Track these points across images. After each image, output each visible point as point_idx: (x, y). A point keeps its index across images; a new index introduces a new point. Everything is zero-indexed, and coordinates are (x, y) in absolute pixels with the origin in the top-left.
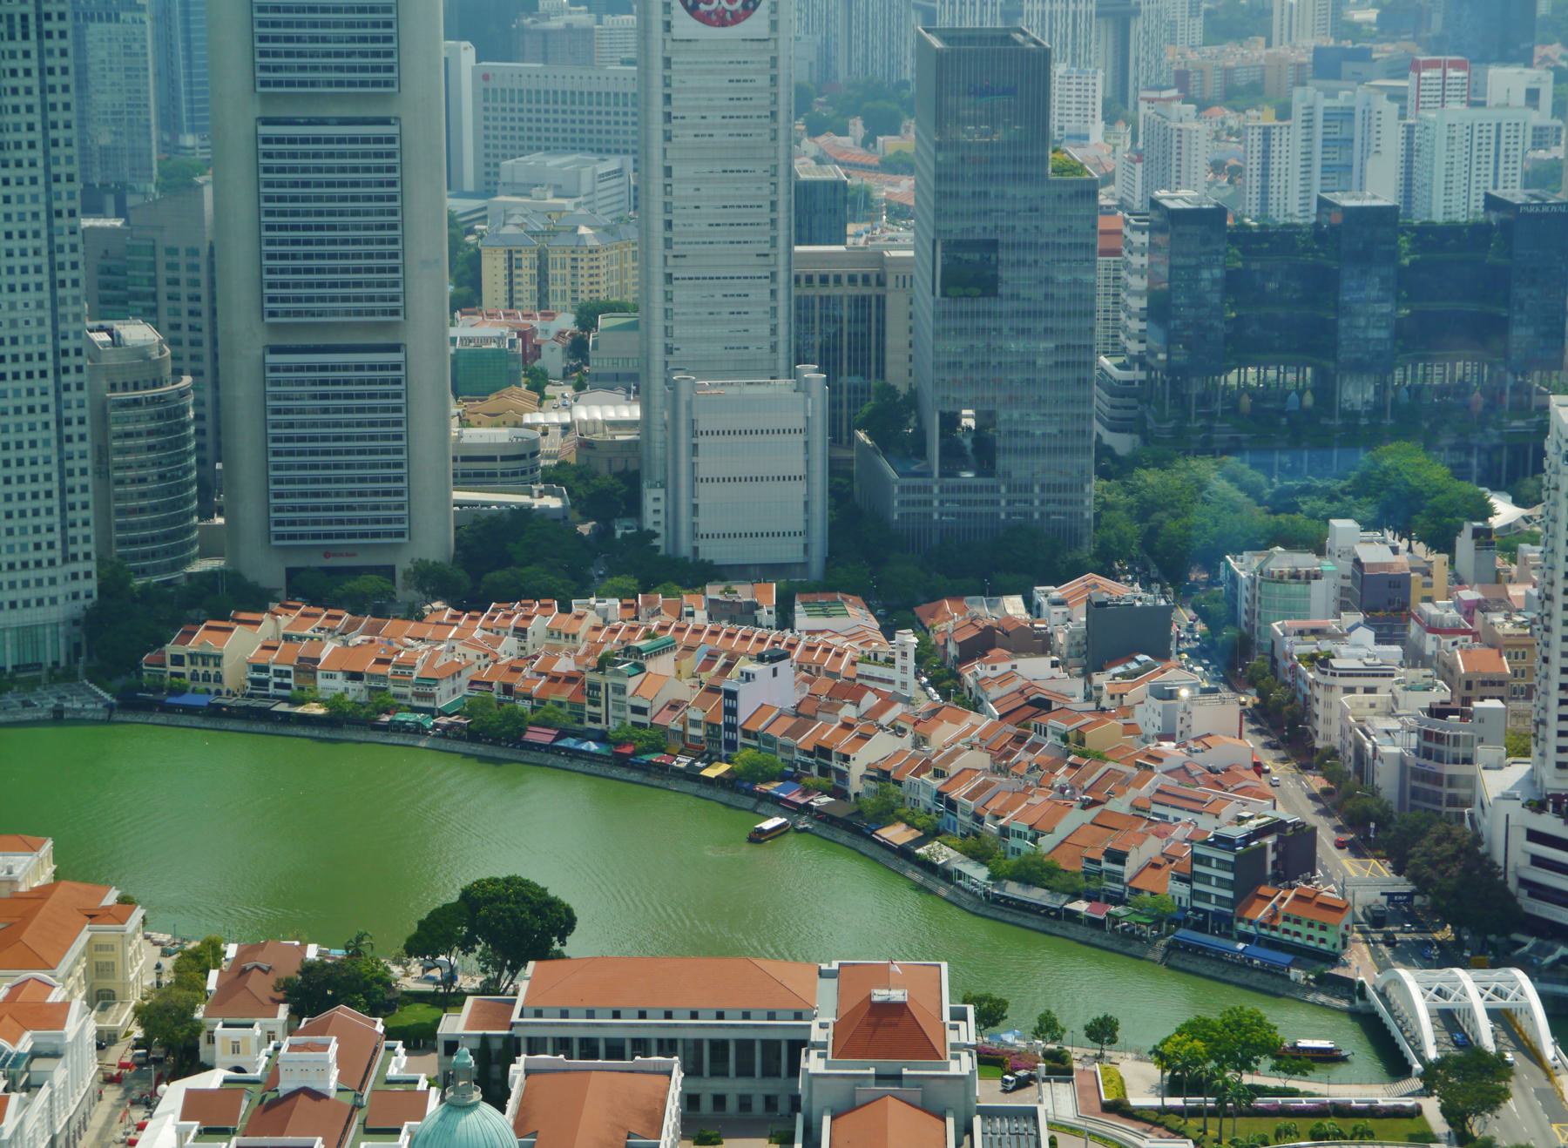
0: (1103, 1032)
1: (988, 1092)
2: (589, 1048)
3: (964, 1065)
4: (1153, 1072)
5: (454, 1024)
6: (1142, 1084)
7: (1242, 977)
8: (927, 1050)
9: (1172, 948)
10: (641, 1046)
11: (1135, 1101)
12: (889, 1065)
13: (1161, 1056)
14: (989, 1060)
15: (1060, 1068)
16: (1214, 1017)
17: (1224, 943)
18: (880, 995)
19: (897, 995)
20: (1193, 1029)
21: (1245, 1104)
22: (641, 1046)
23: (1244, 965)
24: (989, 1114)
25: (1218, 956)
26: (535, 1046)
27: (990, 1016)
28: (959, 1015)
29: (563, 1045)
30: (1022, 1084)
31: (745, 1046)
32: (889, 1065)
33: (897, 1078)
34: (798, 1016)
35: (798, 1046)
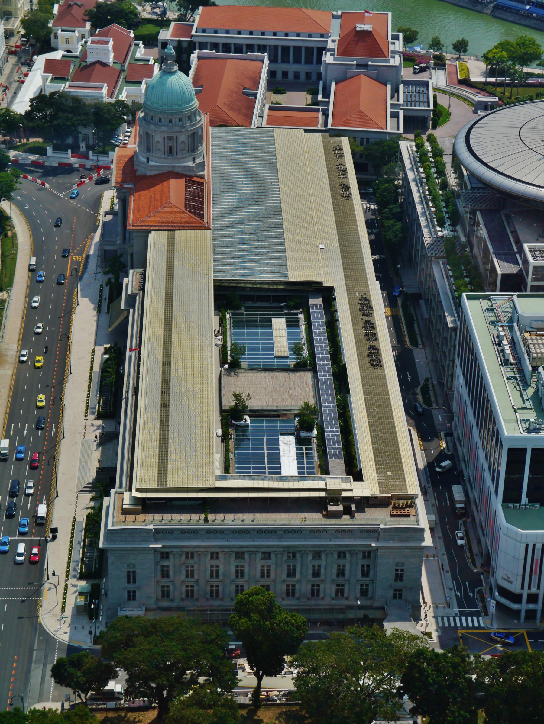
0: (461, 47)
1: (407, 74)
2: (226, 48)
3: (396, 61)
4: (483, 66)
5: (165, 35)
6: (477, 71)
7: (527, 22)
8: (381, 54)
9: (496, 8)
10: (250, 48)
11: (473, 79)
12: (362, 60)
13: (486, 58)
14: (408, 59)
15: (440, 63)
16: (513, 40)
17: (520, 5)
18: (360, 27)
19: (367, 27)
20: (502, 46)
21: (523, 82)
22: (250, 48)
23: (528, 16)
24: (407, 83)
25: (517, 12)
26: (202, 46)
27: (410, 39)
28: (395, 38)
29: (215, 46)
30: (423, 70)
31: (297, 49)
32: (362, 60)
33: (366, 66)
34: (322, 36)
35: (322, 50)
